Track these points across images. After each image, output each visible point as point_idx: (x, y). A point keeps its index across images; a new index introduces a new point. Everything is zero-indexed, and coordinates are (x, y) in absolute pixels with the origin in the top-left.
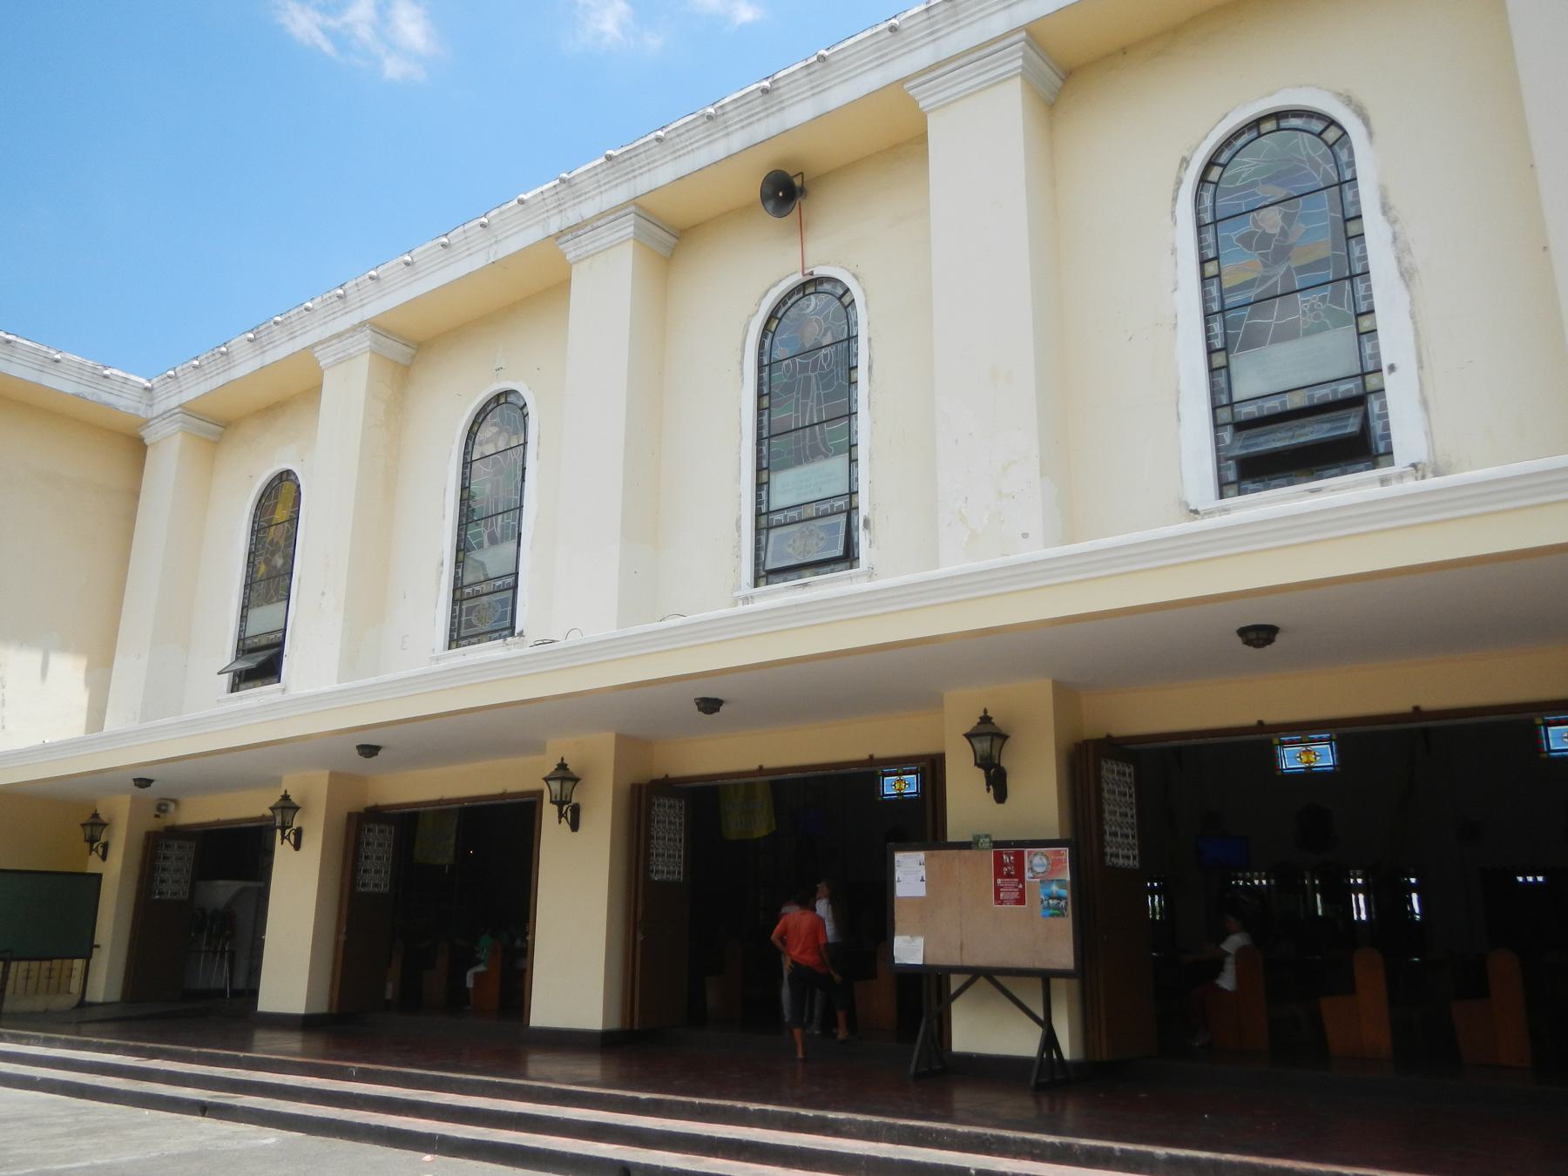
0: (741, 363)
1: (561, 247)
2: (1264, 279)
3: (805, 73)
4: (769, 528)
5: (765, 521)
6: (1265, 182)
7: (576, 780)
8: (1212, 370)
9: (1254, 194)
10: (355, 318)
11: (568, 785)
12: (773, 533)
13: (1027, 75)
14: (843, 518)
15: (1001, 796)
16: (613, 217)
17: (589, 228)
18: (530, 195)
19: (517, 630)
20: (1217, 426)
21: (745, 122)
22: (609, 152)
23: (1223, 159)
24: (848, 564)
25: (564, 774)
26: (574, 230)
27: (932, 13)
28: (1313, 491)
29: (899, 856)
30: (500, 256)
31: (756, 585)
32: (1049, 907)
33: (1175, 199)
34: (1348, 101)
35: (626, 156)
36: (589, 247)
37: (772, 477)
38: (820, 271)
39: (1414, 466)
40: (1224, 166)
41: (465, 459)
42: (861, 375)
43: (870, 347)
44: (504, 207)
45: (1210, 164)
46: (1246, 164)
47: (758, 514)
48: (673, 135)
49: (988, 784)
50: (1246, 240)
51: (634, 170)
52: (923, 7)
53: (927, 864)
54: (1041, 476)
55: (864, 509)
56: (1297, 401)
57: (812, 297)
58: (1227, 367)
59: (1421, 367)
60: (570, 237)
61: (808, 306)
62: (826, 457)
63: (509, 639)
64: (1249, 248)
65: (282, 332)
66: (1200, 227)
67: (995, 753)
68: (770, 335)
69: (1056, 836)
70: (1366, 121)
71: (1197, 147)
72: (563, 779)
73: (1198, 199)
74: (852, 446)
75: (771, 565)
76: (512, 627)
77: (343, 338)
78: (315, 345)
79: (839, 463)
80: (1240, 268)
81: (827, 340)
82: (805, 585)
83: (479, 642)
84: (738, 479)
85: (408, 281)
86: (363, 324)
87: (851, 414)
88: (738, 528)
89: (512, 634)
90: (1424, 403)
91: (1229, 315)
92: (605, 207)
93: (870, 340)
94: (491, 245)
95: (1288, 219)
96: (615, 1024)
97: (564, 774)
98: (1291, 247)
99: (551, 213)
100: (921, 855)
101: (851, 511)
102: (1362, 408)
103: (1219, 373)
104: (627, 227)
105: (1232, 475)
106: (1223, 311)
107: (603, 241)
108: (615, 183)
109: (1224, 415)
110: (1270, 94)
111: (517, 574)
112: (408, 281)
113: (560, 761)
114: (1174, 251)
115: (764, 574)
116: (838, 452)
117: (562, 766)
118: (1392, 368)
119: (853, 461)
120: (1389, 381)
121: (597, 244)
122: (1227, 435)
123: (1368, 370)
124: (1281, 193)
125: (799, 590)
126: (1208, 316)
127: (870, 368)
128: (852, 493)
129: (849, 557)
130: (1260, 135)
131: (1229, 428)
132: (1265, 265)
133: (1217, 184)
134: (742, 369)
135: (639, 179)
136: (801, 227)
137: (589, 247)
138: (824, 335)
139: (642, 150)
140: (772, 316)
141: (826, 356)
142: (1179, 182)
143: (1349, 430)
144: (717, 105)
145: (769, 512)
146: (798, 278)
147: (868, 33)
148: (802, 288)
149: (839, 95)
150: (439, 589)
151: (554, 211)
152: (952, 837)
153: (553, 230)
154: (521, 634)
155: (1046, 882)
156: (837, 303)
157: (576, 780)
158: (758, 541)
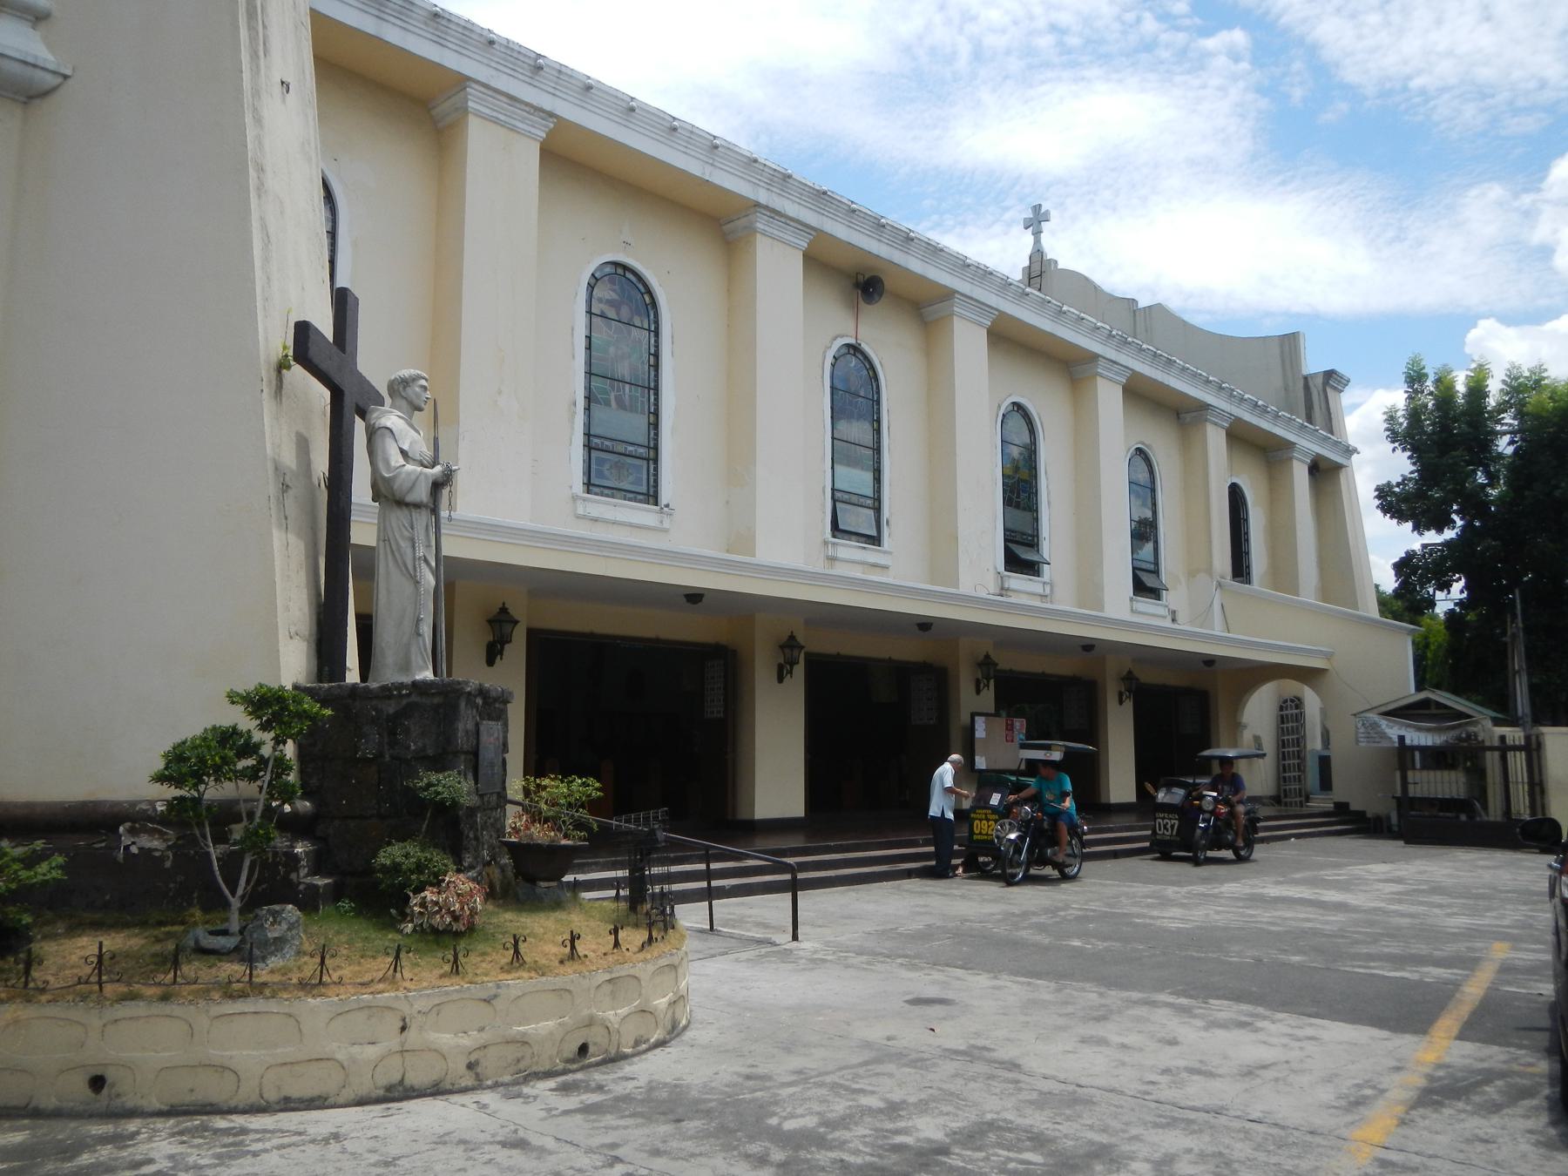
0: (823, 377)
10: (547, 103)
17: (783, 220)
26: (775, 213)
38: (864, 347)
53: (985, 723)
60: (768, 214)
65: (426, 24)
77: (518, 105)
78: (478, 82)
82: (864, 548)
83: (613, 497)
85: (620, 121)
86: (551, 115)
107: (786, 237)
112: (620, 121)
121: (781, 235)
129: (876, 540)
139: (836, 202)
146: (852, 341)
150: (573, 428)
155: (1019, 733)
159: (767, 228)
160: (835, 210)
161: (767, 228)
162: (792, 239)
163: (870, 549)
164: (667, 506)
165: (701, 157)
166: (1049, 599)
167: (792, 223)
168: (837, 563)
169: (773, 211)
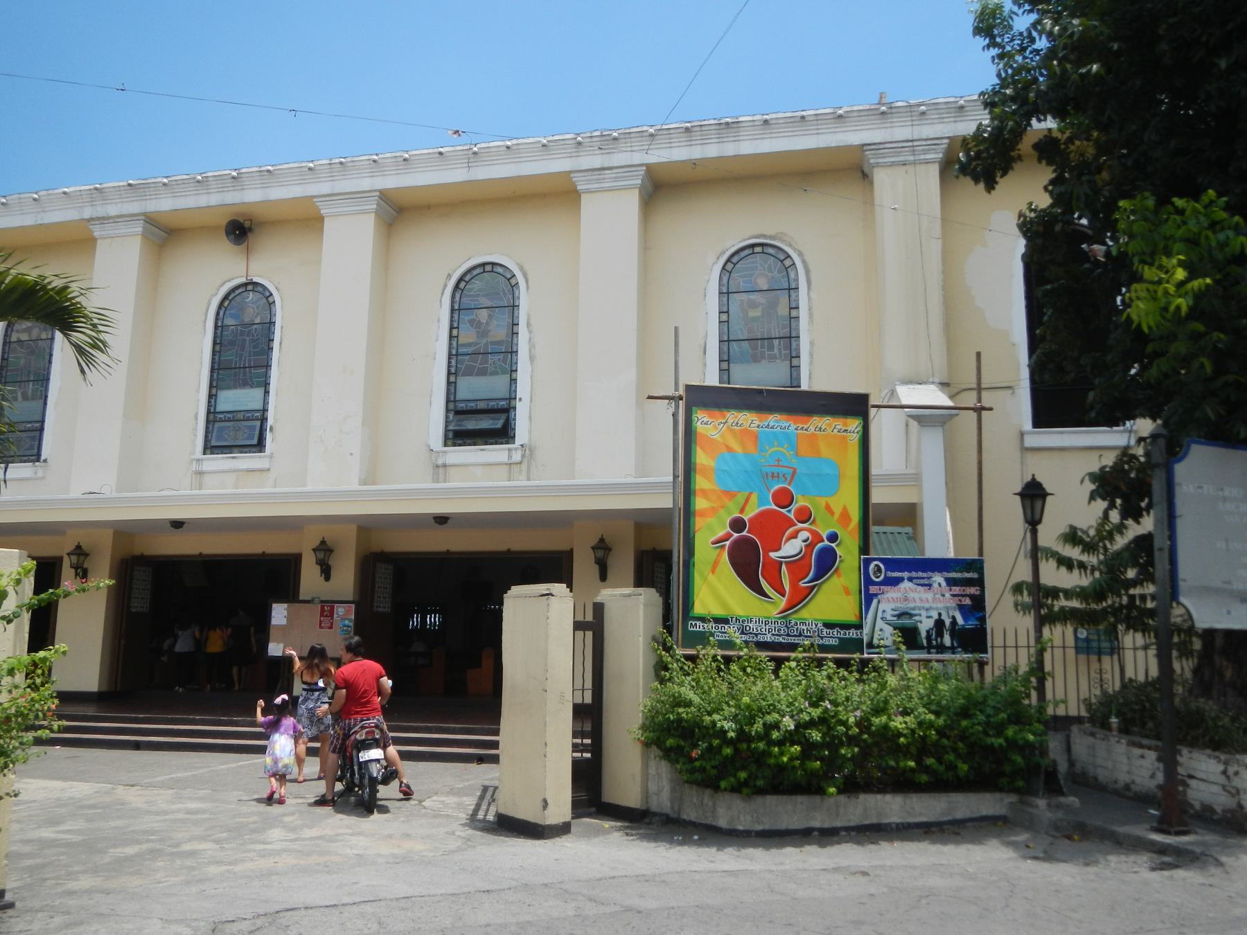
0: (205, 322)
1: (91, 227)
2: (476, 344)
3: (259, 174)
4: (215, 421)
5: (213, 416)
6: (484, 296)
7: (86, 555)
8: (449, 383)
9: (478, 301)
11: (82, 558)
12: (217, 425)
13: (378, 214)
14: (258, 423)
15: (327, 578)
16: (128, 219)
17: (112, 221)
18: (72, 189)
19: (43, 458)
20: (447, 410)
21: (220, 190)
22: (131, 182)
23: (467, 278)
24: (259, 448)
25: (79, 551)
27: (332, 166)
28: (482, 450)
29: (274, 606)
30: (46, 221)
31: (204, 453)
32: (343, 630)
33: (442, 294)
34: (521, 269)
35: (141, 186)
36: (110, 232)
37: (219, 392)
38: (256, 280)
39: (522, 446)
40: (467, 282)
41: (5, 339)
42: (276, 345)
43: (282, 332)
44: (51, 192)
45: (461, 279)
46: (477, 285)
47: (209, 412)
48: (174, 183)
49: (321, 573)
50: (471, 322)
51: (146, 196)
52: (328, 162)
53: (288, 609)
54: (363, 425)
55: (270, 422)
56: (482, 405)
57: (251, 293)
58: (455, 383)
59: (531, 402)
60: (97, 222)
61: (248, 297)
62: (252, 387)
63: (37, 463)
64: (472, 326)
66: (452, 310)
67: (326, 559)
68: (223, 309)
69: (351, 599)
70: (527, 282)
71: (455, 270)
72: (79, 555)
73: (453, 296)
74: (266, 385)
75: (214, 443)
76: (38, 455)
79: (258, 393)
80: (467, 336)
81: (258, 321)
82: (234, 457)
84: (198, 391)
87: (268, 366)
88: (196, 419)
89: (38, 460)
90: (530, 418)
91: (460, 358)
92: (125, 212)
93: (282, 327)
94: (39, 212)
95: (490, 317)
96: (104, 689)
97: (79, 551)
98: (490, 331)
99: (85, 204)
100: (286, 605)
101: (264, 420)
102: (506, 414)
103: (451, 385)
104: (138, 228)
105: (451, 435)
106: (457, 355)
107: (121, 231)
108: (131, 199)
109: (451, 406)
110: (491, 254)
111: (43, 422)
113: (77, 544)
114: (439, 320)
115: (209, 448)
116: (258, 386)
117: (79, 547)
118: (520, 399)
119: (267, 392)
120: (519, 405)
122: (451, 416)
123: (512, 398)
124: (489, 304)
125: (230, 460)
126: (450, 356)
127: (281, 343)
128: (265, 410)
129: (260, 446)
130: (484, 272)
131: (452, 412)
132: (478, 337)
133: (462, 290)
134: (205, 326)
135: (148, 202)
136: (248, 252)
137: (110, 232)
138: (256, 317)
139: (152, 185)
140: (226, 298)
141: (256, 329)
142: (445, 286)
143: (497, 427)
144: (204, 175)
145: (215, 412)
146: (243, 280)
147: (296, 165)
148: (246, 285)
149: (279, 193)
151: (87, 204)
152: (301, 598)
153: (87, 216)
154: (45, 461)
155: (343, 619)
156: (265, 300)
157: (86, 555)
158: (207, 428)
159: (103, 233)
160: (155, 191)
161: (103, 233)
162: (125, 231)
163: (240, 457)
164: (45, 461)
165: (33, 211)
166: (524, 467)
167: (120, 220)
168: (205, 475)
169: (98, 219)
